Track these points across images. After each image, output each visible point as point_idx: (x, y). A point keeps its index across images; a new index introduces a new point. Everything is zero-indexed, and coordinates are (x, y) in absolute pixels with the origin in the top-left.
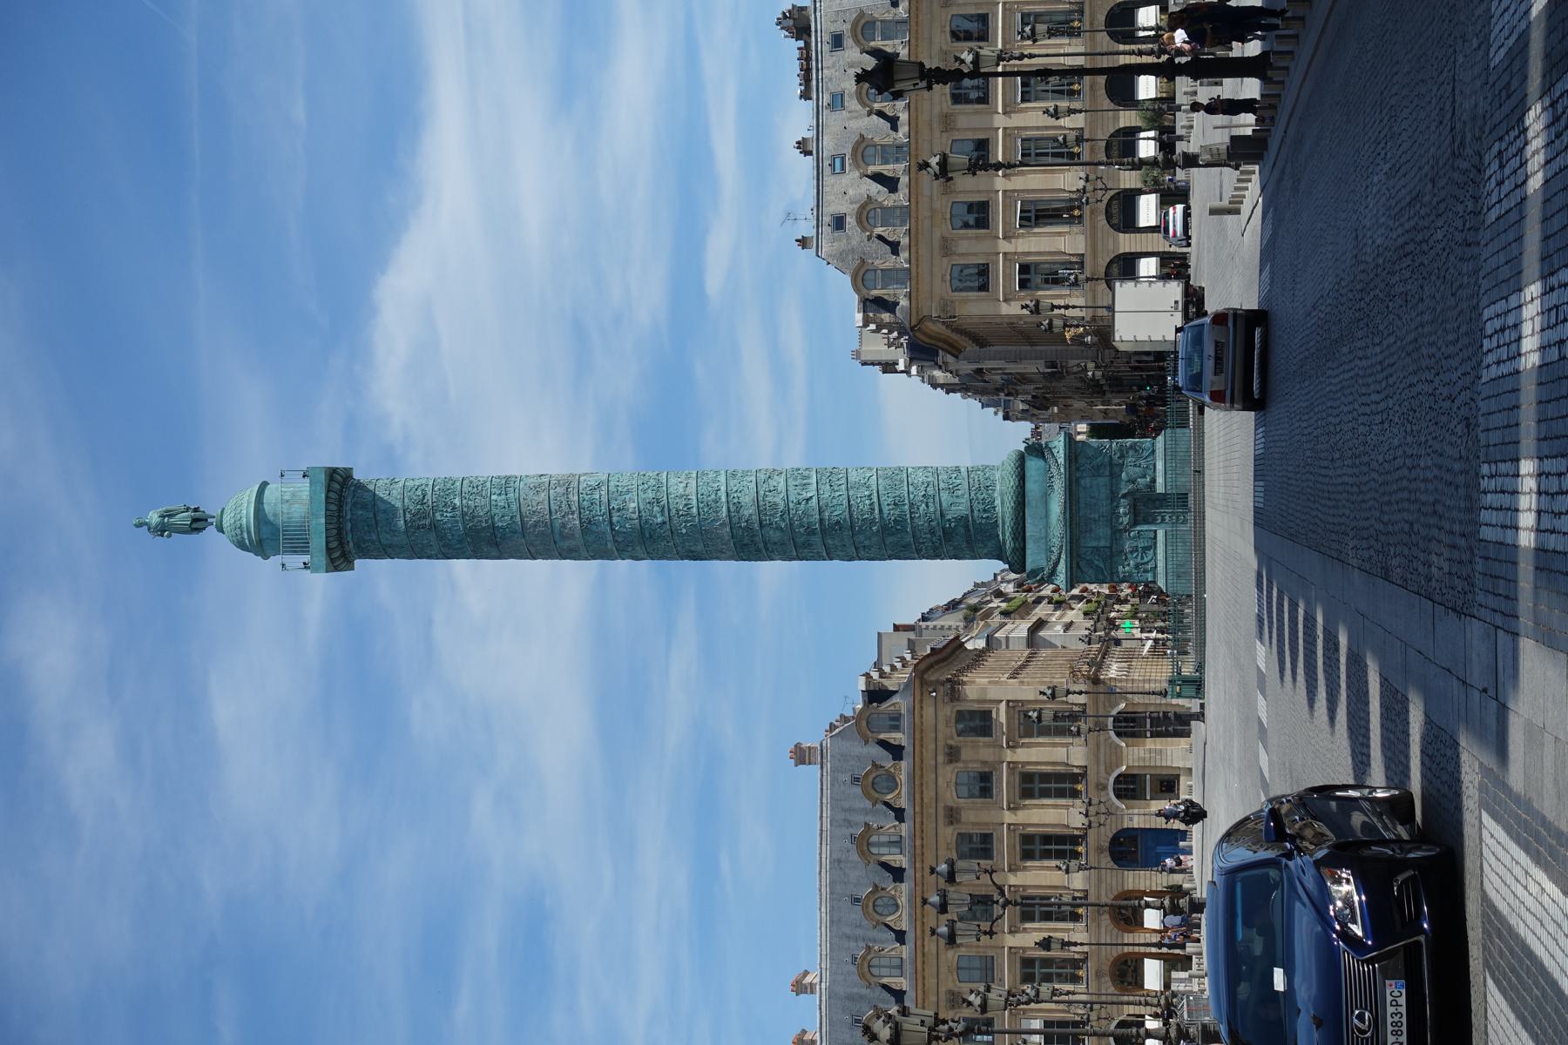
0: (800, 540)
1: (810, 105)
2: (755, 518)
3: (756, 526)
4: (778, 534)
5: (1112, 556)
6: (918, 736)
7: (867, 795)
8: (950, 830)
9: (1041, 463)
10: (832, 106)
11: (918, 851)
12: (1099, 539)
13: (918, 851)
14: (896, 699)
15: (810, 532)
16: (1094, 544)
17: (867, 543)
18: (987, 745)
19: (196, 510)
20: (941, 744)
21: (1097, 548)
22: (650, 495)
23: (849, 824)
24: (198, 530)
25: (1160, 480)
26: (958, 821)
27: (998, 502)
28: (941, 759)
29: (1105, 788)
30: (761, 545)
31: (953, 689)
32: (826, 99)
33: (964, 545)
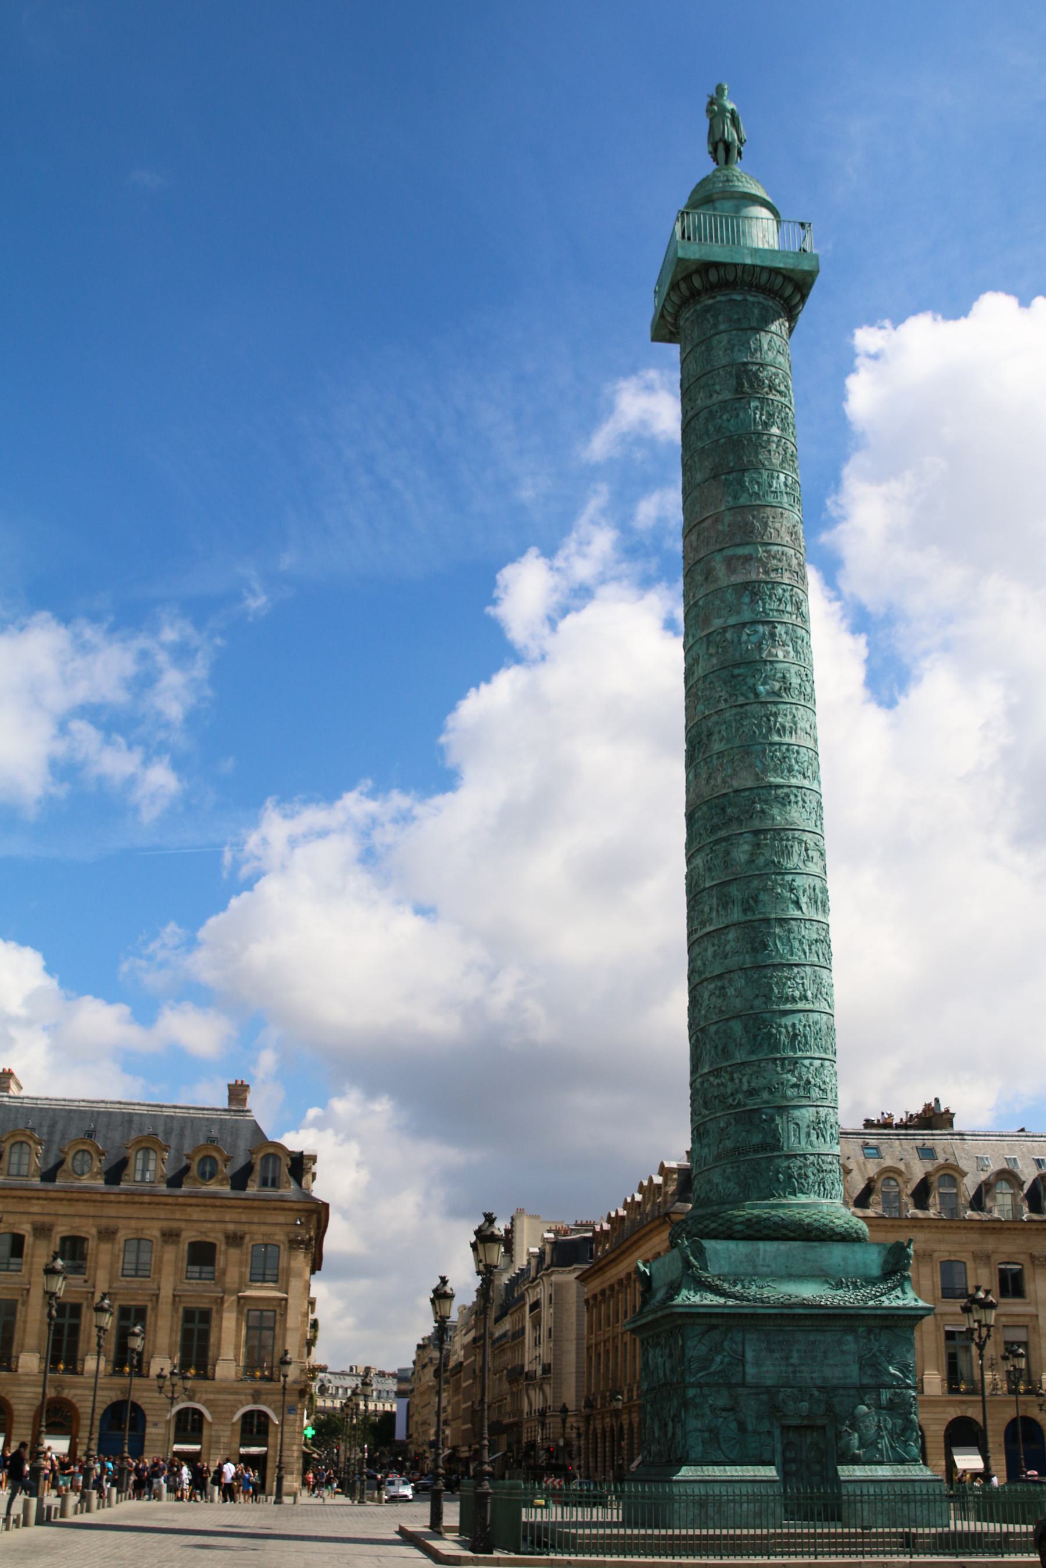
0: (734, 891)
1: (859, 1126)
2: (768, 824)
3: (757, 824)
4: (743, 858)
5: (730, 1386)
6: (256, 1204)
7: (197, 1149)
8: (157, 1233)
9: (875, 1271)
10: (866, 1146)
11: (137, 1199)
12: (757, 1364)
13: (137, 1199)
14: (293, 1186)
15: (750, 904)
16: (749, 1355)
17: (731, 991)
18: (241, 1276)
19: (740, 153)
20: (246, 1228)
21: (742, 1361)
22: (795, 681)
23: (168, 1133)
24: (714, 153)
25: (859, 1472)
26: (165, 1242)
27: (802, 1199)
28: (231, 1227)
29: (191, 1398)
30: (723, 833)
31: (302, 1242)
32: (873, 1142)
33: (729, 1144)
